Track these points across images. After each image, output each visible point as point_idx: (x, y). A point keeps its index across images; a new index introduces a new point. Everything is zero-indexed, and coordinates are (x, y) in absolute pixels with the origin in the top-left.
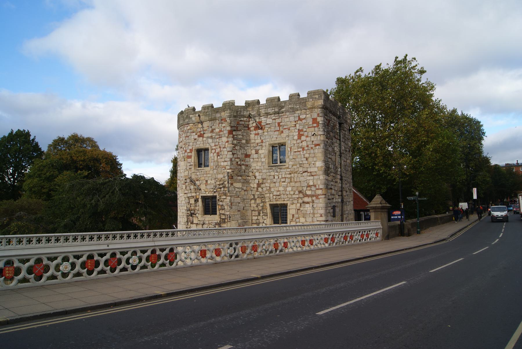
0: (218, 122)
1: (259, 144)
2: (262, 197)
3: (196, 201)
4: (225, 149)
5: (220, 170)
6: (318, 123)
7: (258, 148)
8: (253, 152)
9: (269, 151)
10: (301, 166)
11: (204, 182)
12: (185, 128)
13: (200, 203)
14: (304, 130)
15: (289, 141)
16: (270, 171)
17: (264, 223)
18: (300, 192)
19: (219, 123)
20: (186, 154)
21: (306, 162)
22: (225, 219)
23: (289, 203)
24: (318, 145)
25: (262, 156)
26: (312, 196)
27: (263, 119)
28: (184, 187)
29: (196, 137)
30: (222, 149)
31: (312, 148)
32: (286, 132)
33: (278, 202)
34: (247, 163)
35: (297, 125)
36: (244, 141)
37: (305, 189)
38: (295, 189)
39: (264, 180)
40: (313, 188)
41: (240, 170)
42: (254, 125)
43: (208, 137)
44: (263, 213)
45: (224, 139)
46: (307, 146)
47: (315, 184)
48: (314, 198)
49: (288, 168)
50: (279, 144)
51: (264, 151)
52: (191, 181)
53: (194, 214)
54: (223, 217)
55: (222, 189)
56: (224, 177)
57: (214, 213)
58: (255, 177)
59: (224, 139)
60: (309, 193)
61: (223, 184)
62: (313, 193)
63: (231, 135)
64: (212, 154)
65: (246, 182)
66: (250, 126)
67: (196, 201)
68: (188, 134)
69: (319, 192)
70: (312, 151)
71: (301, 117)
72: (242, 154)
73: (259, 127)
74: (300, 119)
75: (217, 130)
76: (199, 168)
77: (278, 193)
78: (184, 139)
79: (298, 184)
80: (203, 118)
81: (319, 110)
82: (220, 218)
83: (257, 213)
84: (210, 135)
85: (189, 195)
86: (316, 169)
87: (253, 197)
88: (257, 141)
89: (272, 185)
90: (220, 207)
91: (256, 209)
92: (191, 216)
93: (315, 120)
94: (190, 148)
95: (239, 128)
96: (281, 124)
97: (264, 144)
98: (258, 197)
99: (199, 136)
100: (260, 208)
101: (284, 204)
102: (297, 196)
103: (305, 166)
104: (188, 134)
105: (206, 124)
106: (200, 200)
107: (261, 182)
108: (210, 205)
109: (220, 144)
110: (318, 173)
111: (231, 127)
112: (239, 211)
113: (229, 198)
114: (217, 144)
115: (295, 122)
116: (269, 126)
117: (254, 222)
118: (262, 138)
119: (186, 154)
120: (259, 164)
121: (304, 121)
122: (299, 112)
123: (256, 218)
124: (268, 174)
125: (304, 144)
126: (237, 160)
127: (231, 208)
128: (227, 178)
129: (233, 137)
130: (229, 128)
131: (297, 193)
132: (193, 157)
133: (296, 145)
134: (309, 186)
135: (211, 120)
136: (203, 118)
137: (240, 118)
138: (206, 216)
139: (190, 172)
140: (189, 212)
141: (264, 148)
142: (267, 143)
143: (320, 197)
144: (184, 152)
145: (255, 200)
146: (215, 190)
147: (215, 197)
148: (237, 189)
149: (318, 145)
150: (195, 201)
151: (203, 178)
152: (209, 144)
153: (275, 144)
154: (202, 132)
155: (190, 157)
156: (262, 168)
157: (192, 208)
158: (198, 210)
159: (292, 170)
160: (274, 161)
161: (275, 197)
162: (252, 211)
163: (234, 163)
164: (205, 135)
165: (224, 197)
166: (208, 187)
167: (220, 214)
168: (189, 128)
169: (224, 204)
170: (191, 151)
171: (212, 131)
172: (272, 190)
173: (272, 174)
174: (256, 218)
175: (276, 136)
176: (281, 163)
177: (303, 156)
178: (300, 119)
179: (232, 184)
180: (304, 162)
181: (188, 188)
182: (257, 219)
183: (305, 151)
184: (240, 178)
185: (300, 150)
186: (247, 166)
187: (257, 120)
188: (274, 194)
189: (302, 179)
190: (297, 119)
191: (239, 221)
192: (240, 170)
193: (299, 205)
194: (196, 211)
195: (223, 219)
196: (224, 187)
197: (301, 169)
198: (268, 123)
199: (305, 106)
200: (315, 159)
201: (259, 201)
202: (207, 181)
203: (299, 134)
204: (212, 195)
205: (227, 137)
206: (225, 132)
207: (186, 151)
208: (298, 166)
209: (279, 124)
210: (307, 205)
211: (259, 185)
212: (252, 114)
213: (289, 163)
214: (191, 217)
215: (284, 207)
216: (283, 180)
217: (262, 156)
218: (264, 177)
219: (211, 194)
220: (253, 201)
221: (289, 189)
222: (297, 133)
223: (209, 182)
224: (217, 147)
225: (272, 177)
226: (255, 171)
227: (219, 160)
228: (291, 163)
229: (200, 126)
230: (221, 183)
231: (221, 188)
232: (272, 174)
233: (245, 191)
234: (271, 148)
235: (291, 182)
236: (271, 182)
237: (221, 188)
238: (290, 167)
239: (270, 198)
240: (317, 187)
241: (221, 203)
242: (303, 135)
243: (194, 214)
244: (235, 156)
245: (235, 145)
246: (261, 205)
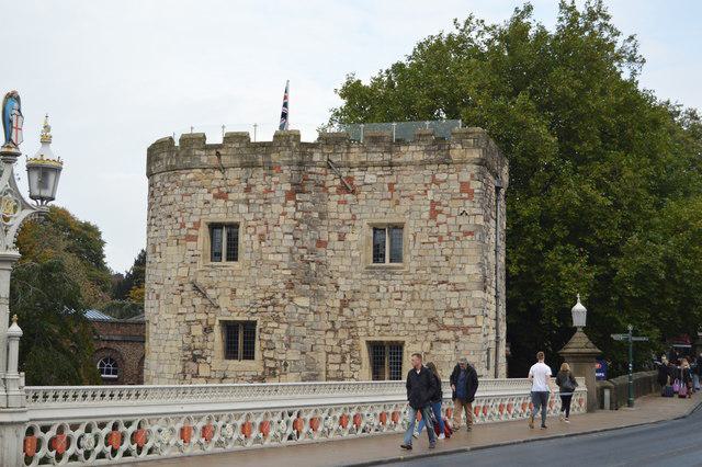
0: (262, 171)
1: (347, 223)
2: (350, 326)
3: (208, 330)
4: (279, 229)
5: (265, 269)
6: (471, 193)
7: (343, 229)
8: (334, 236)
9: (368, 238)
10: (435, 272)
11: (228, 292)
12: (183, 177)
13: (217, 336)
14: (445, 203)
15: (412, 223)
16: (370, 276)
17: (353, 377)
18: (431, 320)
19: (266, 175)
20: (184, 232)
21: (446, 264)
22: (274, 369)
23: (407, 340)
24: (471, 233)
25: (354, 246)
26: (455, 329)
27: (357, 173)
28: (177, 300)
29: (210, 197)
30: (270, 228)
31: (458, 238)
32: (405, 204)
33: (384, 339)
34: (321, 259)
35: (430, 193)
36: (316, 215)
37: (441, 314)
38: (420, 313)
39: (358, 296)
40: (458, 315)
41: (307, 275)
42: (338, 182)
43: (237, 202)
44: (351, 357)
46: (449, 234)
47: (462, 306)
48: (459, 333)
49: (408, 273)
50: (389, 224)
51: (360, 238)
52: (196, 288)
53: (200, 357)
54: (272, 364)
55: (270, 309)
56: (275, 284)
57: (249, 355)
58: (337, 287)
59: (277, 208)
60: (449, 322)
61: (271, 298)
62: (457, 323)
63: (292, 202)
64: (247, 237)
65: (317, 296)
66: (327, 185)
67: (208, 330)
68: (190, 190)
69: (468, 322)
70: (458, 245)
71: (437, 176)
72: (312, 239)
73: (347, 187)
74: (434, 181)
75: (260, 188)
76: (214, 263)
77: (386, 321)
78: (179, 198)
79: (425, 306)
80: (226, 160)
81: (475, 167)
82: (265, 367)
83: (338, 358)
84: (243, 196)
85: (189, 318)
86: (465, 279)
87: (330, 326)
88: (342, 216)
89: (374, 304)
90: (264, 345)
91: (338, 350)
92: (195, 361)
93: (464, 186)
94: (197, 220)
95: (307, 188)
96: (396, 186)
97: (357, 224)
98: (342, 327)
99: (216, 197)
100: (346, 348)
101: (397, 342)
102: (426, 328)
103: (443, 271)
104: (190, 190)
105: (232, 174)
106: (217, 330)
107: (349, 296)
108: (240, 339)
109: (266, 216)
110: (468, 287)
111: (293, 184)
112: (303, 353)
113: (285, 326)
114: (260, 216)
115: (426, 185)
116: (369, 188)
117: (331, 375)
118: (354, 211)
119: (184, 232)
120: (347, 262)
121: (443, 186)
122: (434, 167)
123: (337, 367)
124: (365, 282)
125: (443, 230)
126: (303, 251)
127: (288, 346)
128: (282, 286)
129: (295, 206)
130: (288, 187)
131: (425, 321)
132: (200, 240)
133: (426, 229)
134: (449, 310)
135: (243, 166)
136: (226, 160)
137: (309, 167)
138: (228, 362)
139: (192, 270)
140: (189, 353)
141: (357, 231)
142: (365, 222)
143: (470, 331)
144: (178, 226)
145: (336, 331)
146: (254, 310)
147: (255, 323)
148: (300, 310)
149: (471, 233)
150: (205, 330)
151: (226, 284)
153: (382, 224)
154: (224, 190)
155: (194, 239)
156: (353, 269)
157: (197, 344)
158: (212, 350)
159: (416, 277)
160: (378, 255)
161: (378, 328)
162: (328, 353)
163: (296, 256)
164: (230, 196)
165: (276, 325)
166: (237, 302)
167: (264, 359)
168: (191, 176)
169: (274, 338)
170: (197, 226)
172: (373, 313)
173: (375, 282)
174: (337, 367)
175: (384, 210)
176: (391, 261)
177: (439, 253)
178: (434, 181)
179: (291, 299)
180: (441, 264)
181: (187, 303)
182: (339, 370)
183: (443, 244)
184: (307, 287)
185: (432, 239)
186: (321, 264)
187: (345, 174)
188: (377, 322)
189: (436, 295)
190: (428, 181)
191: (304, 374)
192: (307, 275)
193: (427, 345)
194: (207, 352)
195: (270, 369)
196: (274, 305)
197: (434, 277)
198: (368, 180)
199: (449, 157)
200: (463, 259)
201: (342, 335)
202: (234, 291)
203: (433, 209)
204: (246, 319)
205: (284, 205)
206: (278, 194)
207: (183, 226)
208: (429, 270)
209: (391, 186)
211: (344, 303)
212: (334, 161)
214: (192, 366)
216: (398, 295)
217: (354, 246)
218: (357, 287)
220: (331, 335)
221: (409, 313)
222: (429, 208)
223: (239, 292)
224: (259, 222)
225: (374, 289)
226: (336, 274)
227: (264, 250)
228: (414, 264)
229: (218, 174)
230: (267, 295)
231: (266, 307)
232: (375, 282)
233: (315, 313)
234: (372, 231)
235: (413, 300)
236: (371, 299)
237: (266, 307)
238: (413, 271)
239: (367, 330)
240: (466, 313)
241: (266, 337)
242: (440, 212)
243: (200, 357)
244: (299, 243)
245: (301, 221)
246: (350, 341)
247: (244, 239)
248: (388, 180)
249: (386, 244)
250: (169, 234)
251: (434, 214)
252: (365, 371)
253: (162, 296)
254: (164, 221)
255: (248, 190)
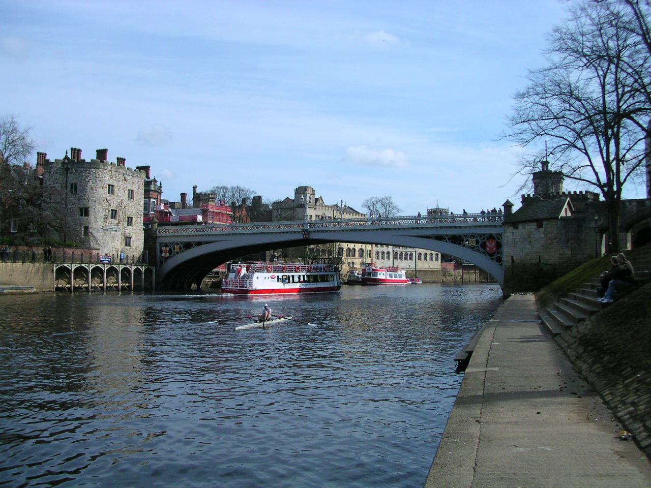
2: (125, 213)
45: (121, 183)
51: (127, 192)
59: (121, 183)
60: (140, 213)
67: (109, 211)
85: (106, 208)
152: (115, 183)
160: (129, 198)
171: (116, 177)
210: (139, 219)
211: (125, 207)
213: (135, 199)
215: (131, 218)
219: (115, 209)
247: (116, 190)
248: (132, 179)
249: (131, 194)
250: (100, 185)
251: (138, 188)
252: (126, 224)
253: (97, 201)
254: (98, 182)
255: (116, 177)
